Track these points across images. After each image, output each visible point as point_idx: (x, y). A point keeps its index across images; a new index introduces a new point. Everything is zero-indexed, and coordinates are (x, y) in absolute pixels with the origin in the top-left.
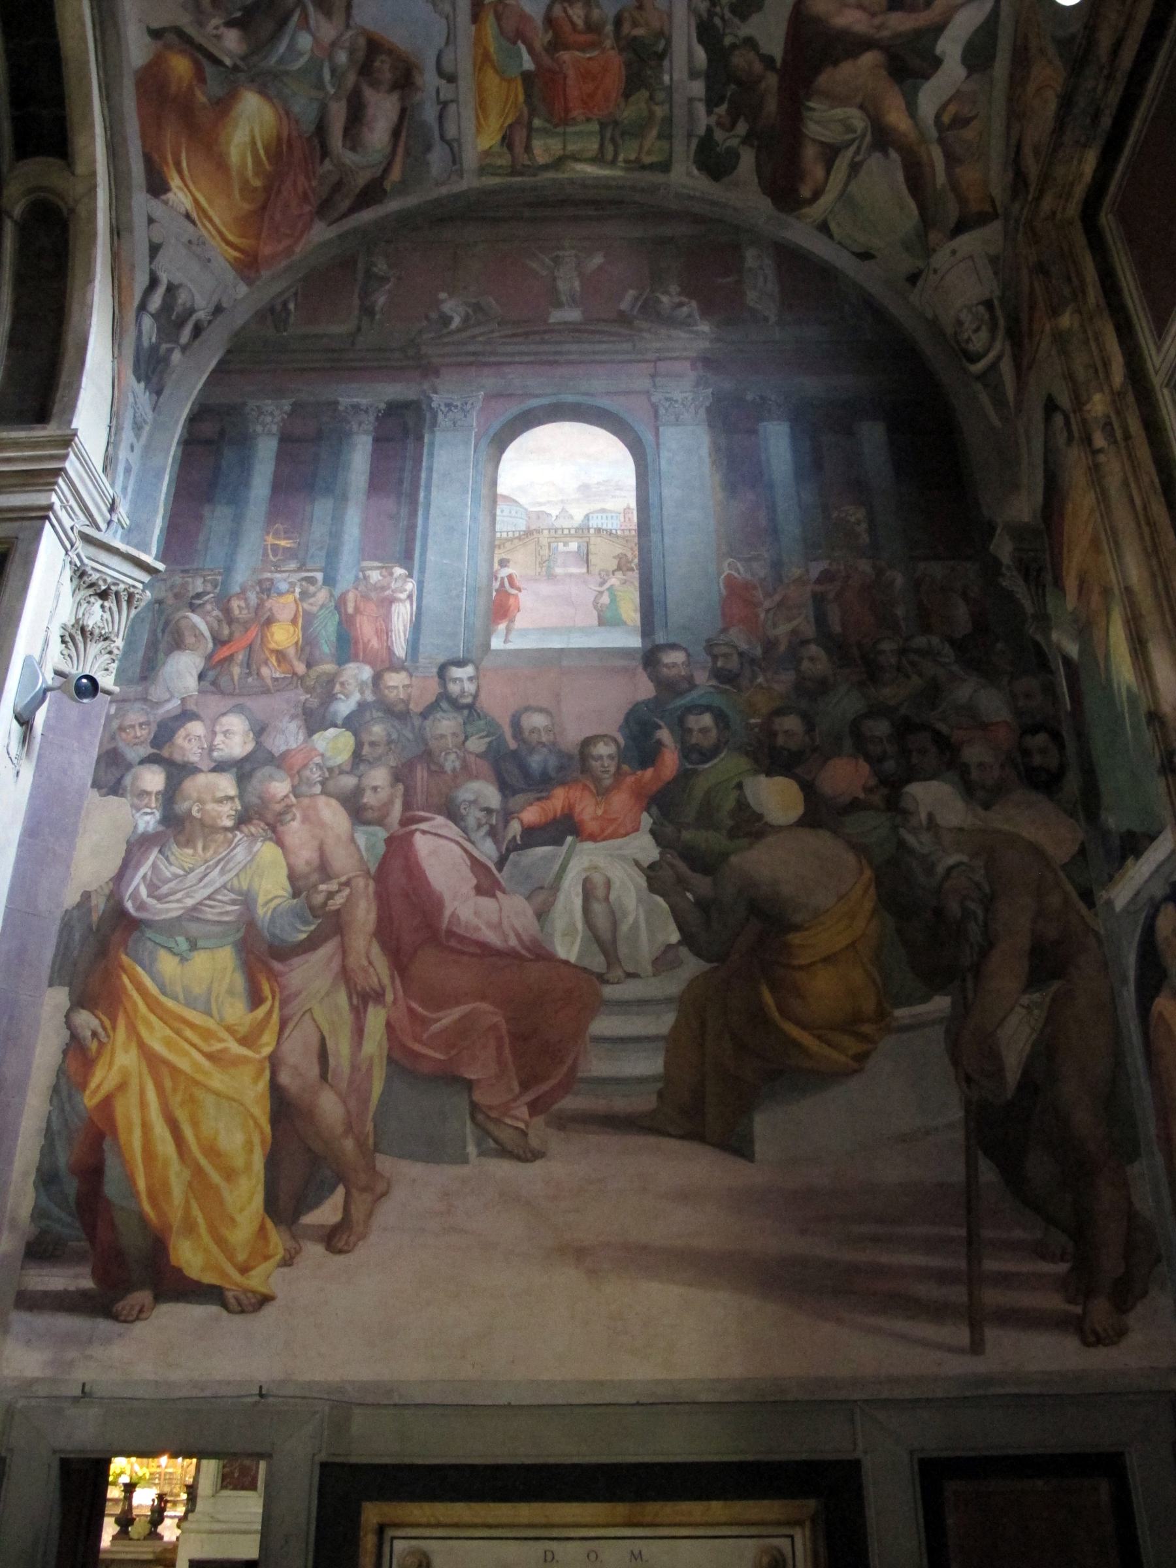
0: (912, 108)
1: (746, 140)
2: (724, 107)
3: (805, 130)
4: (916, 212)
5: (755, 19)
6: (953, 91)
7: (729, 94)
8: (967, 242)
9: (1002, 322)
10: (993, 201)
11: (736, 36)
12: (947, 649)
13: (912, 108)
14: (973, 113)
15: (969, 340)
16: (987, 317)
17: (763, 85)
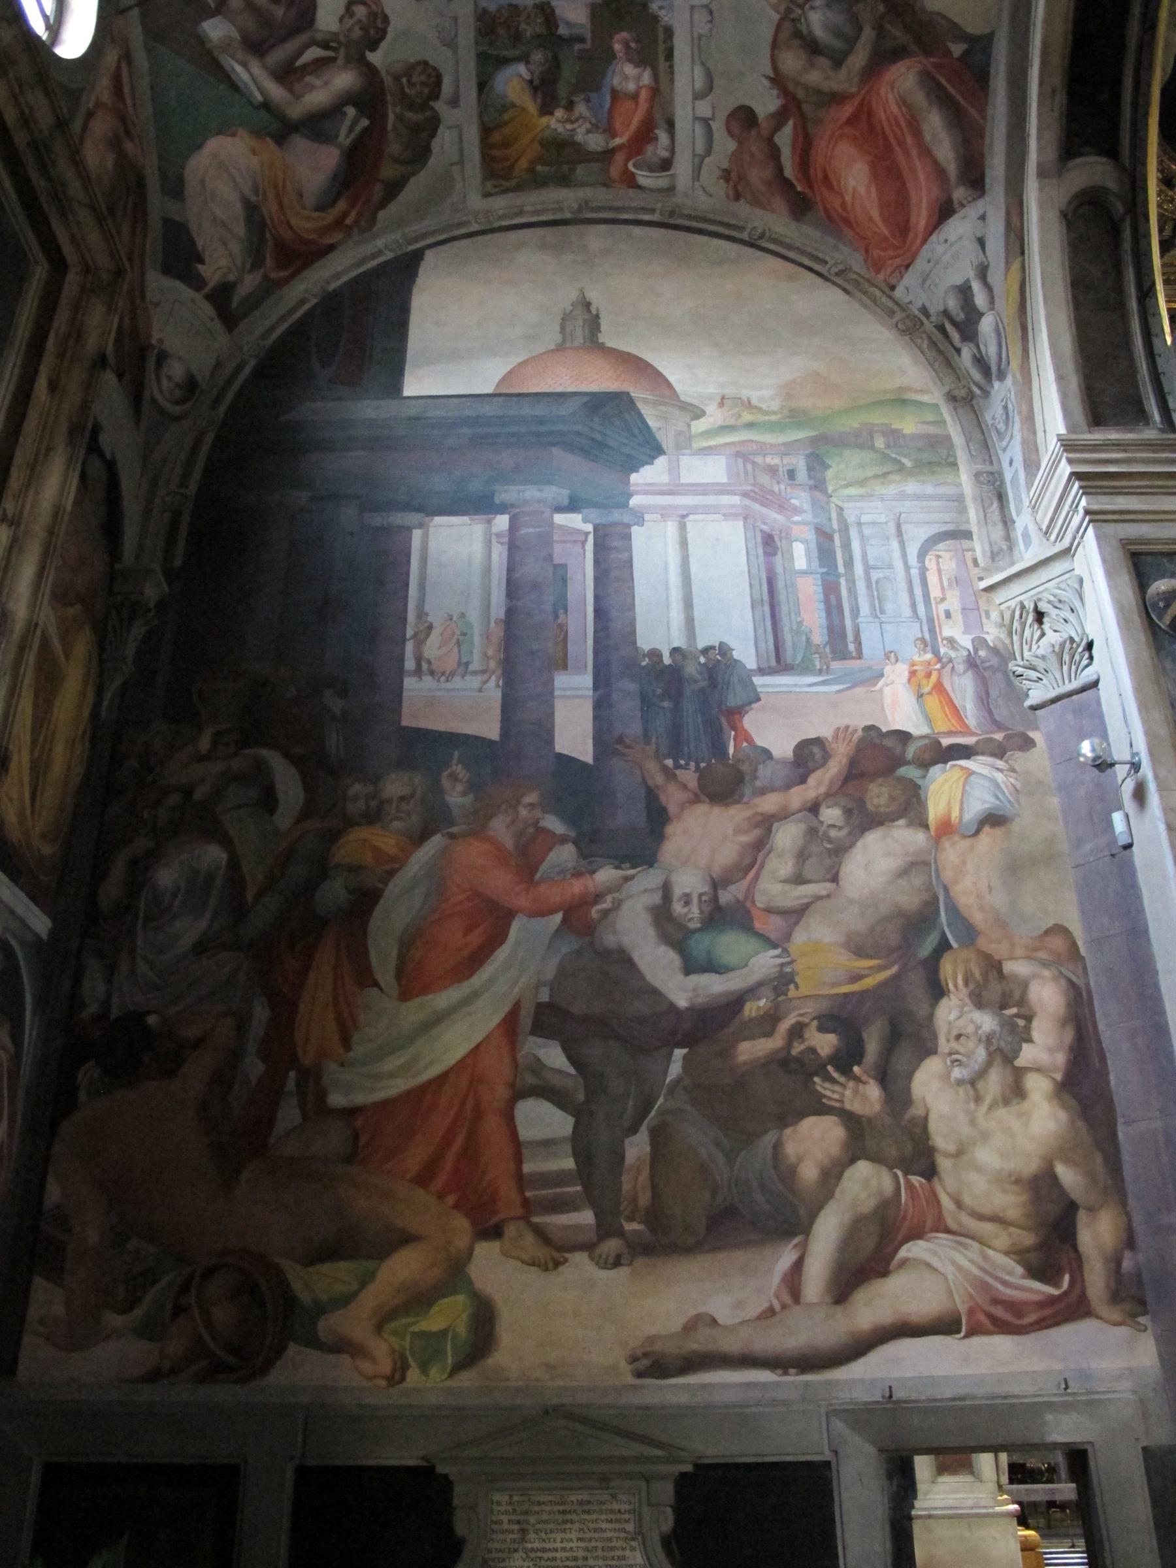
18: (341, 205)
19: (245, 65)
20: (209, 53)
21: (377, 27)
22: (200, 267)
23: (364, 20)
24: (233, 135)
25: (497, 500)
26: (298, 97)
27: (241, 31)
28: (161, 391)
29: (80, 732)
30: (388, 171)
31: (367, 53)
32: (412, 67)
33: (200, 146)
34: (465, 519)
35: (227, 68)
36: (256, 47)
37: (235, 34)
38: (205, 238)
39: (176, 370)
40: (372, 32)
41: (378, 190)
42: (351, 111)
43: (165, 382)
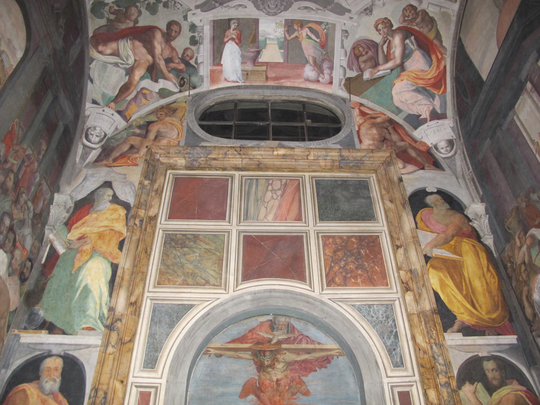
0: (142, 78)
1: (109, 20)
2: (117, 8)
3: (120, 40)
4: (116, 94)
5: (148, 13)
6: (152, 90)
7: (121, 9)
8: (117, 117)
9: (103, 143)
10: (130, 118)
11: (141, 7)
12: (32, 214)
13: (142, 78)
14: (149, 99)
15: (92, 135)
16: (102, 137)
17: (128, 21)
18: (434, 57)
19: (379, 71)
20: (371, 80)
21: (386, 23)
22: (421, 117)
23: (383, 26)
24: (395, 84)
25: (523, 81)
26: (395, 58)
27: (370, 68)
28: (443, 154)
29: (485, 270)
30: (431, 36)
31: (393, 29)
32: (403, 14)
33: (392, 97)
34: (521, 97)
35: (377, 77)
36: (376, 65)
37: (370, 69)
38: (414, 110)
39: (442, 144)
40: (388, 25)
41: (435, 42)
42: (407, 41)
43: (442, 151)
